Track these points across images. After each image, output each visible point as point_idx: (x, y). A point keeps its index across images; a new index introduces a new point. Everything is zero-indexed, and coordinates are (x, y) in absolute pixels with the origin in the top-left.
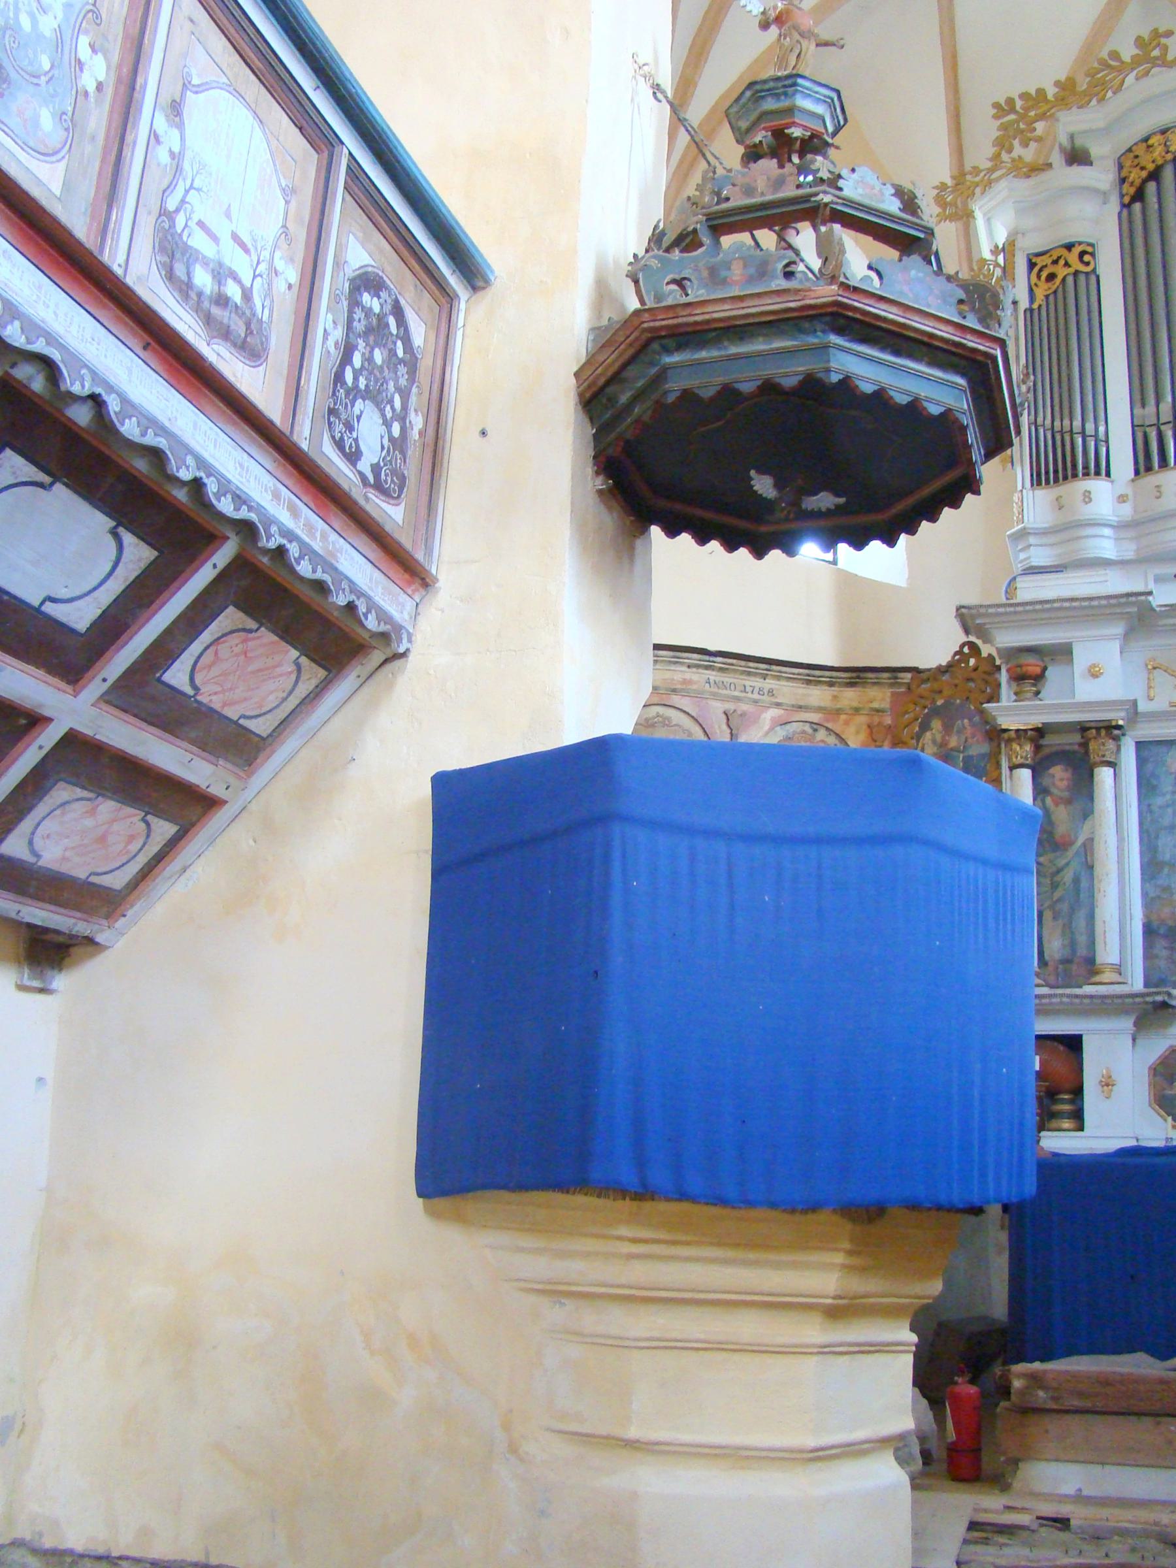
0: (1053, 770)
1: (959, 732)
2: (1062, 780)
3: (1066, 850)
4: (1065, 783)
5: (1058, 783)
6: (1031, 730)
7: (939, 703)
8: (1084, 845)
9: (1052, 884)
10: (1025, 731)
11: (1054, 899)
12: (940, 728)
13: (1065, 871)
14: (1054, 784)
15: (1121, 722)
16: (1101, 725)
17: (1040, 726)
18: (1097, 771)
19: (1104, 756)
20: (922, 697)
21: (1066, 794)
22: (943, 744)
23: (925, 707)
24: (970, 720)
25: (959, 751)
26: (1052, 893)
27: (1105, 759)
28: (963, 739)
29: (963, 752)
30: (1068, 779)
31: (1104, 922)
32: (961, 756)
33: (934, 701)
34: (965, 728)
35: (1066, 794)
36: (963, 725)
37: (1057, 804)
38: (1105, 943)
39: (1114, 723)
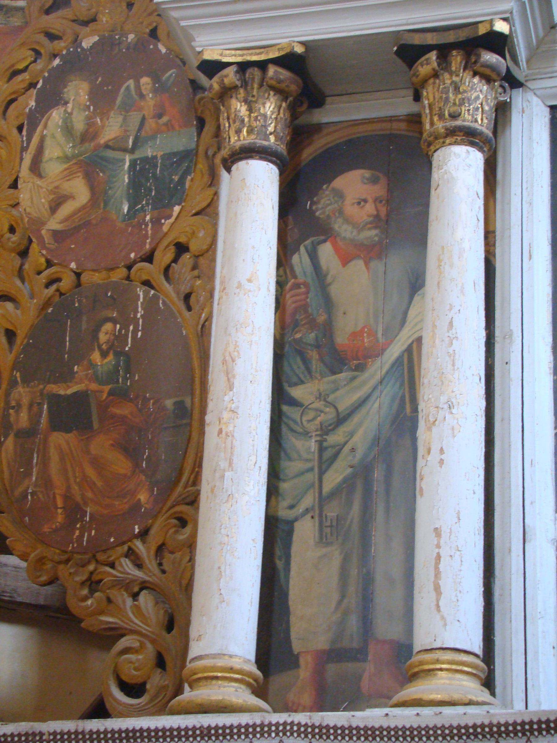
0: (339, 182)
1: (127, 108)
2: (362, 202)
3: (360, 368)
4: (370, 208)
5: (350, 209)
6: (277, 61)
7: (86, 44)
8: (409, 350)
9: (321, 449)
10: (262, 65)
11: (327, 488)
12: (84, 97)
13: (356, 419)
14: (341, 212)
15: (501, 27)
16: (451, 38)
17: (299, 49)
18: (438, 157)
19: (454, 116)
20: (52, 37)
21: (372, 234)
22: (86, 137)
23: (55, 56)
24: (156, 78)
25: (125, 150)
26: (321, 473)
27: (459, 123)
28: (135, 118)
29: (132, 151)
30: (377, 200)
31: (437, 532)
32: (128, 158)
33: (76, 41)
34: (142, 96)
35: (372, 234)
36: (138, 87)
37: (345, 260)
38: (437, 589)
39: (482, 30)
